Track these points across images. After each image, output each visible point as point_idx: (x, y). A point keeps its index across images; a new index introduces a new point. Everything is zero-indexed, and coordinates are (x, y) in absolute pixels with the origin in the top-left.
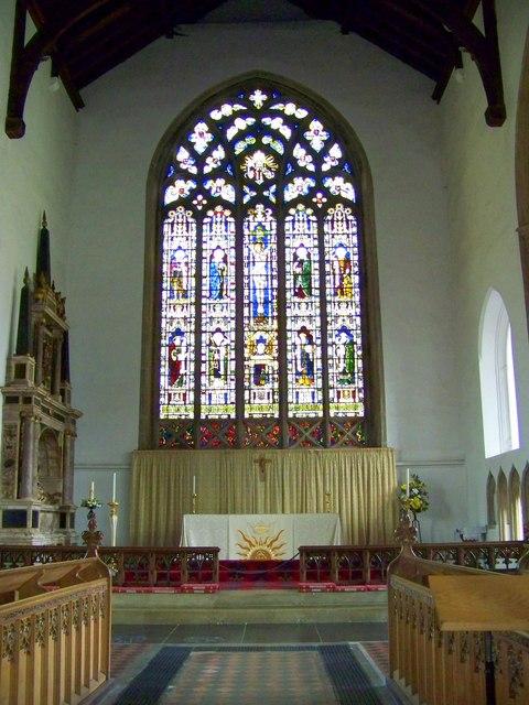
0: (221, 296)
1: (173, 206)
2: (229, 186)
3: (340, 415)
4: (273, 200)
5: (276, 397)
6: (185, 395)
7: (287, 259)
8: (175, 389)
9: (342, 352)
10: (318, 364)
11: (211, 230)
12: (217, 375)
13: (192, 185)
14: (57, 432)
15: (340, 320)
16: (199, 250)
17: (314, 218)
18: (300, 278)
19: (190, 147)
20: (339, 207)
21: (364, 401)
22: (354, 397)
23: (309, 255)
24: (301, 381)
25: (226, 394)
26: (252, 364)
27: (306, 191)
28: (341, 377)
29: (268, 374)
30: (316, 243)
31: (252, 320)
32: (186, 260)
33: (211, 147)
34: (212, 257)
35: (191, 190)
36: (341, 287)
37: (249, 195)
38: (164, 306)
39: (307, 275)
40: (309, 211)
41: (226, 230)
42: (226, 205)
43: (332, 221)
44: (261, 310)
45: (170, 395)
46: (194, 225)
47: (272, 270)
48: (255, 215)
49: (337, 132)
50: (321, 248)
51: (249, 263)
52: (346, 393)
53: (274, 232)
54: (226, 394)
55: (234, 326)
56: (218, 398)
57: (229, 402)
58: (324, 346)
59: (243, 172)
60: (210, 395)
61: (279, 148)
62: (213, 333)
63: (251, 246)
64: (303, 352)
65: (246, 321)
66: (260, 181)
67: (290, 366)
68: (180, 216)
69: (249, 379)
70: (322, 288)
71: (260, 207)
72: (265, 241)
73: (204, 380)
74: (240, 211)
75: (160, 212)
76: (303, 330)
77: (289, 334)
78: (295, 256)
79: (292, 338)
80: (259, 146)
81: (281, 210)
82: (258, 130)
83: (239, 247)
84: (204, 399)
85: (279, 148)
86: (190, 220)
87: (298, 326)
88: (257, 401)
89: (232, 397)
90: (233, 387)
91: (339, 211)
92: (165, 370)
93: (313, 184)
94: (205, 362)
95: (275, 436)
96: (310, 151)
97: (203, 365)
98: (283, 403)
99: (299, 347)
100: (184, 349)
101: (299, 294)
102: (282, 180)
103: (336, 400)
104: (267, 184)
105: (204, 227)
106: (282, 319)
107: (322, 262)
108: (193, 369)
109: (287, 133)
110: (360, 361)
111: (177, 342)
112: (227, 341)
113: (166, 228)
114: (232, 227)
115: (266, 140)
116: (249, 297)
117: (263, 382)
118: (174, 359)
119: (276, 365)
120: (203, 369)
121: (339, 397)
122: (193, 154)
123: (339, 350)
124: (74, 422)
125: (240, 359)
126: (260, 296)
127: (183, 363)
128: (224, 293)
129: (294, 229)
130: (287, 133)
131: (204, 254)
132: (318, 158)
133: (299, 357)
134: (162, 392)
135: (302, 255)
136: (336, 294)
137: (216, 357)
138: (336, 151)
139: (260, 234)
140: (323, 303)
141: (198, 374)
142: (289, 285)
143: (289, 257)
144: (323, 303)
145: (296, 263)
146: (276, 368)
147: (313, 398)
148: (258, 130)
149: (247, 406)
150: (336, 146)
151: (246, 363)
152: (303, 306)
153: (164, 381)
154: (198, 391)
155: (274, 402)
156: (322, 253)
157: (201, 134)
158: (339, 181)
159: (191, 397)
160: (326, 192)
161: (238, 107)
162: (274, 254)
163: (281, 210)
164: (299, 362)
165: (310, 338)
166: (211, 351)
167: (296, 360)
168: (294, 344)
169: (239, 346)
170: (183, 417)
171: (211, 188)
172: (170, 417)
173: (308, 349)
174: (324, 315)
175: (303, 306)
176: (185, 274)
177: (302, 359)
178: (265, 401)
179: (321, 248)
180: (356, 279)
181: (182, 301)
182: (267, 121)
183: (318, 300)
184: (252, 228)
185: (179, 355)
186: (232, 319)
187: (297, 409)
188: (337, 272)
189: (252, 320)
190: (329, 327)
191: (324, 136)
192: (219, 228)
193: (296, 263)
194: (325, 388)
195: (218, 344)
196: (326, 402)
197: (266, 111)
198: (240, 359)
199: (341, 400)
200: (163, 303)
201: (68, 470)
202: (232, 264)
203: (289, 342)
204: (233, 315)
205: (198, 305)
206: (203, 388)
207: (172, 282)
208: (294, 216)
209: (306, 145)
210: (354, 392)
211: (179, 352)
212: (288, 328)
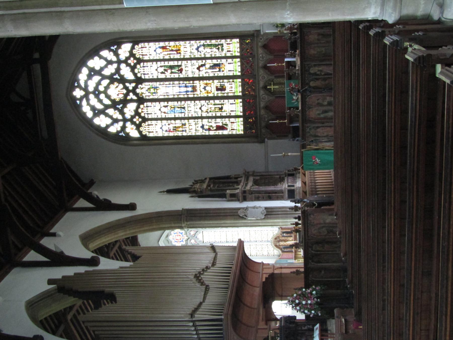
0: (184, 108)
1: (140, 132)
5: (231, 80)
6: (232, 123)
8: (229, 127)
9: (208, 50)
10: (215, 61)
12: (221, 109)
13: (128, 124)
14: (254, 179)
15: (192, 51)
16: (162, 119)
17: (142, 64)
18: (173, 71)
19: (108, 126)
20: (134, 52)
22: (230, 44)
23: (161, 66)
24: (223, 69)
28: (220, 50)
29: (221, 85)
33: (107, 115)
34: (165, 113)
36: (176, 51)
37: (131, 96)
39: (171, 67)
41: (151, 106)
42: (138, 107)
45: (232, 130)
47: (170, 84)
48: (142, 93)
49: (95, 52)
50: (157, 61)
51: (167, 95)
52: (228, 48)
56: (233, 107)
57: (234, 103)
58: (205, 58)
59: (121, 100)
60: (231, 111)
62: (202, 111)
63: (159, 94)
65: (196, 96)
66: (125, 91)
67: (216, 75)
68: (145, 129)
69: (223, 93)
71: (138, 91)
72: (155, 88)
73: (224, 114)
74: (141, 100)
75: (144, 138)
76: (198, 68)
78: (162, 73)
79: (203, 73)
80: (105, 92)
81: (139, 81)
82: (97, 93)
83: (159, 100)
84: (233, 114)
85: (105, 82)
88: (233, 89)
89: (232, 101)
91: (138, 51)
92: (220, 132)
94: (216, 114)
95: (249, 80)
96: (106, 66)
98: (234, 77)
99: (207, 71)
100: (210, 124)
101: (181, 71)
102: (122, 80)
104: (126, 88)
106: (194, 79)
107: (164, 60)
111: (207, 127)
112: (206, 104)
113: (151, 135)
114: (149, 104)
115: (101, 88)
116: (184, 95)
117: (224, 87)
118: (215, 128)
119: (216, 81)
120: (219, 115)
122: (112, 124)
123: (208, 52)
124: (248, 172)
125: (214, 98)
128: (182, 106)
130: (96, 78)
131: (164, 117)
132: (110, 62)
135: (162, 70)
136: (180, 53)
138: (105, 53)
139: (152, 90)
140: (184, 59)
141: (221, 117)
142: (176, 76)
143: (163, 76)
144: (184, 59)
146: (217, 81)
147: (231, 63)
148: (97, 93)
153: (225, 132)
154: (230, 117)
155: (233, 82)
156: (160, 60)
159: (232, 120)
162: (162, 83)
163: (139, 81)
165: (202, 66)
166: (210, 112)
167: (213, 72)
168: (206, 73)
169: (207, 98)
173: (208, 66)
174: (191, 59)
176: (174, 125)
178: (233, 85)
179: (157, 61)
180: (172, 43)
181: (187, 125)
184: (150, 94)
185: (213, 126)
186: (195, 102)
187: (236, 71)
188: (169, 53)
189: (195, 93)
191: (96, 58)
192: (150, 110)
193: (166, 72)
194: (226, 58)
195: (207, 108)
196: (233, 57)
197: (85, 89)
198: (214, 98)
199: (231, 50)
200: (188, 134)
201: (270, 174)
205: (189, 118)
207: (178, 131)
208: (141, 74)
209: (102, 69)
210: (227, 44)
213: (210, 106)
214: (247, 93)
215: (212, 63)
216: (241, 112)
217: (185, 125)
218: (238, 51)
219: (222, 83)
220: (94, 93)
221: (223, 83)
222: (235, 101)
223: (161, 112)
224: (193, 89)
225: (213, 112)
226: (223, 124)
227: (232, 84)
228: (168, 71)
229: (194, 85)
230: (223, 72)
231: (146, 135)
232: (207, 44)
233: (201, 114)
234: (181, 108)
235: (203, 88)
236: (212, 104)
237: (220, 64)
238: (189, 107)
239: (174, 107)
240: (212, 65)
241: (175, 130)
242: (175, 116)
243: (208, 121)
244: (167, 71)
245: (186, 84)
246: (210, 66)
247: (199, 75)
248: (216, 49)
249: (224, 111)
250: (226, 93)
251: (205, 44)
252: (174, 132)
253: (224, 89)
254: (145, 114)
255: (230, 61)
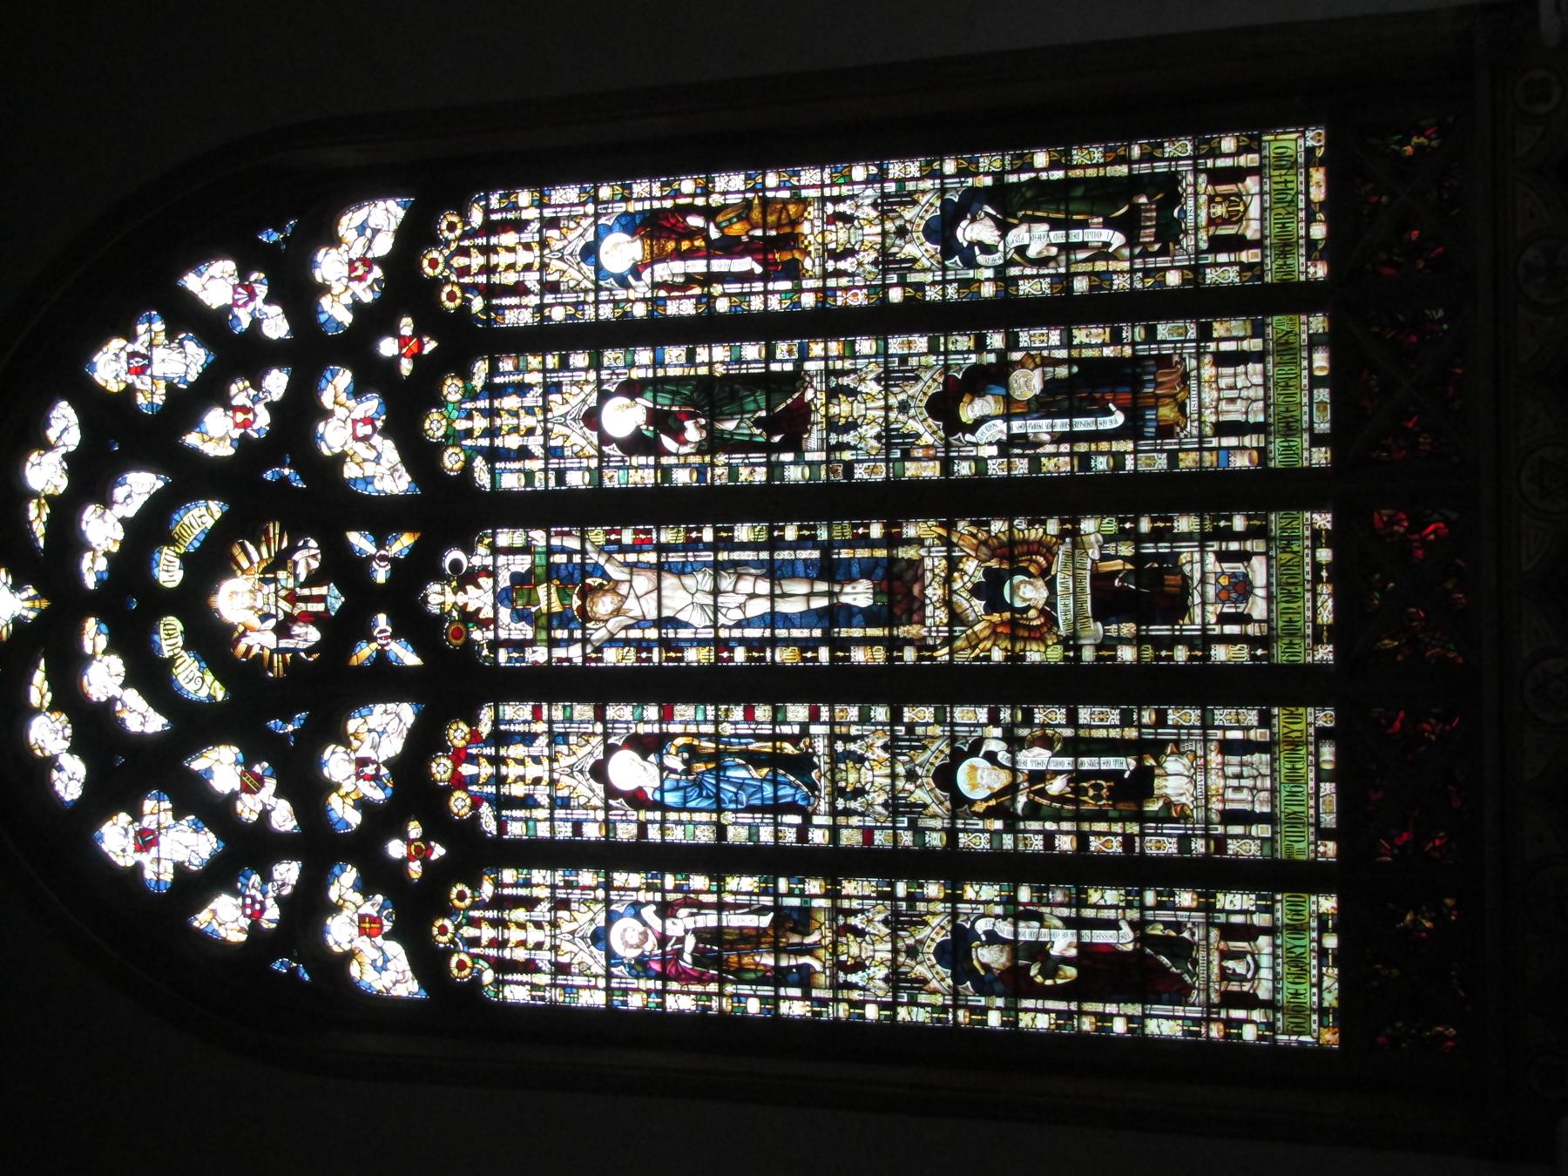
1: (428, 961)
2: (352, 725)
3: (1318, 231)
4: (402, 544)
5: (1239, 523)
6: (1229, 932)
7: (648, 478)
9: (1037, 238)
11: (528, 802)
20: (433, 263)
21: (1253, 130)
22: (1238, 175)
23: (632, 389)
24: (1167, 412)
25: (1227, 747)
26: (1095, 630)
27: (371, 405)
28: (1147, 235)
29: (1138, 559)
30: (579, 359)
31: (902, 631)
32: (648, 913)
34: (637, 799)
35: (365, 887)
38: (843, 1011)
40: (452, 389)
41: (528, 738)
42: (425, 741)
43: (490, 291)
44: (859, 595)
46: (509, 875)
47: (693, 545)
48: (470, 618)
51: (665, 643)
52: (1220, 210)
53: (538, 536)
54: (1227, 747)
55: (926, 713)
60: (1229, 817)
61: (200, 518)
62: (959, 802)
64: (1042, 406)
66: (334, 599)
67: (1101, 464)
70: (767, 328)
76: (943, 408)
77: (964, 469)
78: (637, 444)
84: (1244, 846)
85: (200, 518)
86: (487, 890)
87: (927, 431)
88: (1258, 609)
90: (1193, 716)
93: (344, 378)
94: (1082, 838)
95: (1418, 525)
97: (1095, 844)
99: (1017, 426)
100: (1028, 931)
103: (1246, 256)
105: (516, 830)
107: (657, 331)
108: (1112, 896)
109: (139, 487)
110: (1078, 156)
114: (517, 713)
115: (169, 572)
117: (1172, 580)
121: (1239, 243)
126: (798, 598)
127: (1088, 936)
128: (788, 748)
129: (524, 453)
130: (139, 487)
131: (626, 832)
133: (1061, 425)
134: (1215, 1031)
135: (624, 417)
137: (1057, 786)
139: (546, 598)
143: (641, 474)
145: (668, 442)
146: (1110, 526)
149: (1280, 656)
150: (191, 282)
151: (1088, 655)
152: (842, 408)
153: (1164, 1026)
156: (625, 333)
157: (146, 840)
158: (329, 266)
159: (1235, 902)
160: (371, 320)
161: (39, 689)
164: (1083, 424)
165: (982, 380)
166: (1033, 811)
167: (1072, 437)
168: (1005, 447)
170: (1331, 942)
171: (363, 804)
172: (1330, 999)
173: (1028, 384)
175: (842, 408)
176: (710, 920)
177: (1070, 413)
178: (1258, 571)
180: (731, 185)
182: (92, 570)
183: (817, 349)
184: (525, 631)
186: (896, 718)
187: (1290, 429)
188: (698, 266)
189: (902, 631)
190: (932, 294)
191: (151, 328)
193: (668, 442)
195: (1001, 779)
199: (1252, 231)
200: (829, 1013)
202: (667, 717)
203: (996, 469)
204: (880, 713)
206: (1199, 846)
207: (740, 975)
210: (1217, 176)
211: (1038, 950)
212: (931, 471)
213: (1034, 758)
214: (1389, 643)
215: (1062, 354)
216: (1323, 834)
217: (801, 919)
218: (1311, 244)
219: (1149, 548)
220: (106, 603)
221: (1164, 548)
222: (1265, 721)
223: (611, 792)
224: (890, 593)
225: (1058, 817)
226: (1142, 938)
227: (1244, 556)
228: (689, 424)
229: (907, 553)
230: (1171, 444)
231: (476, 982)
232: (1035, 182)
233: (952, 834)
234: (775, 761)
235: (976, 591)
236: (1047, 742)
237: (1136, 359)
238: (848, 755)
239: (717, 757)
240: (1062, 372)
241: (718, 962)
242: (721, 830)
243: (1011, 901)
244: (678, 434)
245: (827, 548)
246: (1050, 385)
247: (947, 464)
248: (1109, 224)
249: (1164, 817)
250: (1189, 642)
251: (1013, 179)
252: (701, 980)
253: (1177, 607)
254: (476, 802)
255: (1230, 332)
